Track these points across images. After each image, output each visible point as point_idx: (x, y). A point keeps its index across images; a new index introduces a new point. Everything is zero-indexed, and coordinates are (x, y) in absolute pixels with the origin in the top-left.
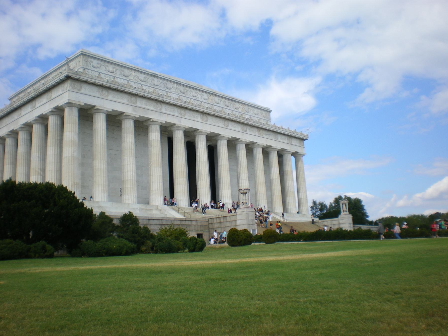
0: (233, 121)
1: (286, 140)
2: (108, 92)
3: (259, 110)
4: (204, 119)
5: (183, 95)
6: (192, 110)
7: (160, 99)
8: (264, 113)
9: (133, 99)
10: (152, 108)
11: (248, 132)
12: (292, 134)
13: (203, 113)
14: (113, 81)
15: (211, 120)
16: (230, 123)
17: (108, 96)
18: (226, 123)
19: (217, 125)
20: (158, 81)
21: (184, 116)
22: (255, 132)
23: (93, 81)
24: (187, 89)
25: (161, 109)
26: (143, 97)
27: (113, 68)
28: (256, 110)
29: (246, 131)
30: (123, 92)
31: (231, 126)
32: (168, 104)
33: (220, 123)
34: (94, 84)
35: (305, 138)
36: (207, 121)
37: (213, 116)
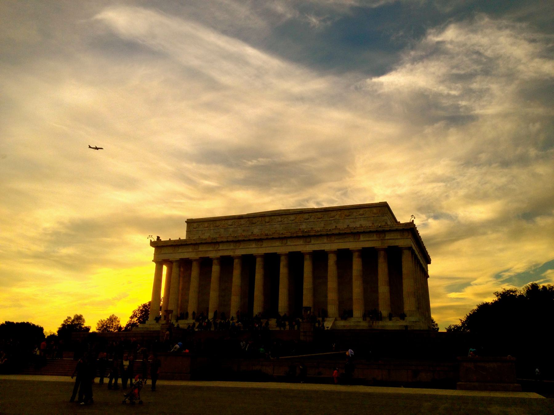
0: (291, 237)
3: (367, 209)
6: (244, 241)
8: (375, 210)
10: (211, 249)
11: (313, 242)
15: (265, 244)
18: (284, 241)
19: (274, 245)
23: (166, 244)
24: (273, 217)
26: (201, 243)
29: (310, 242)
31: (289, 243)
34: (167, 246)
36: (262, 245)
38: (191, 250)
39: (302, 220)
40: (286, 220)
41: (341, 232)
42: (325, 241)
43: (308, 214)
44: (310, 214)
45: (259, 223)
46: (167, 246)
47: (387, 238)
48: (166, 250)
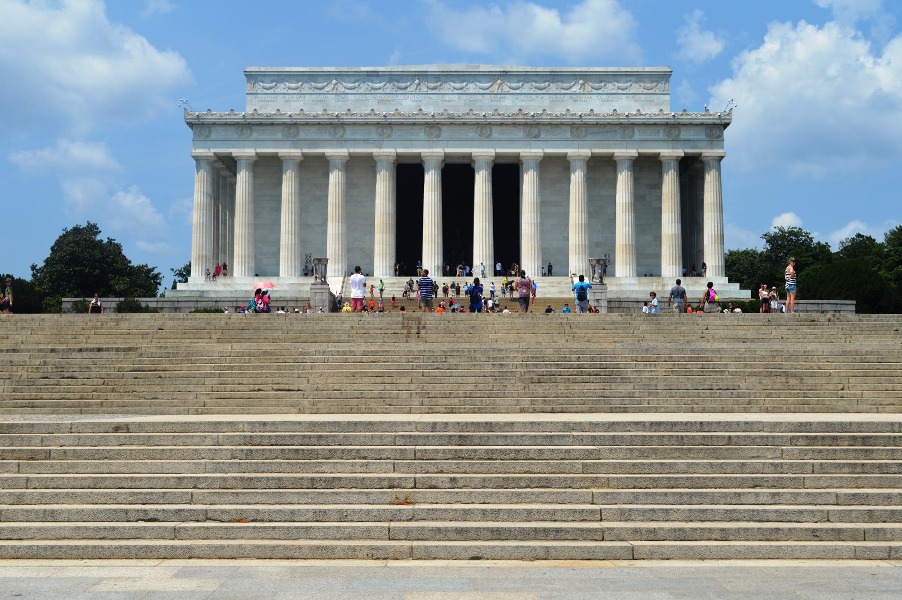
2: (251, 130)
5: (433, 92)
9: (292, 130)
10: (326, 137)
11: (543, 135)
14: (253, 115)
16: (494, 128)
17: (251, 135)
18: (486, 131)
19: (464, 137)
21: (389, 136)
30: (272, 124)
32: (354, 124)
35: (718, 122)
36: (438, 136)
37: (451, 124)
38: (279, 136)
42: (568, 135)
46: (226, 124)
47: (682, 137)
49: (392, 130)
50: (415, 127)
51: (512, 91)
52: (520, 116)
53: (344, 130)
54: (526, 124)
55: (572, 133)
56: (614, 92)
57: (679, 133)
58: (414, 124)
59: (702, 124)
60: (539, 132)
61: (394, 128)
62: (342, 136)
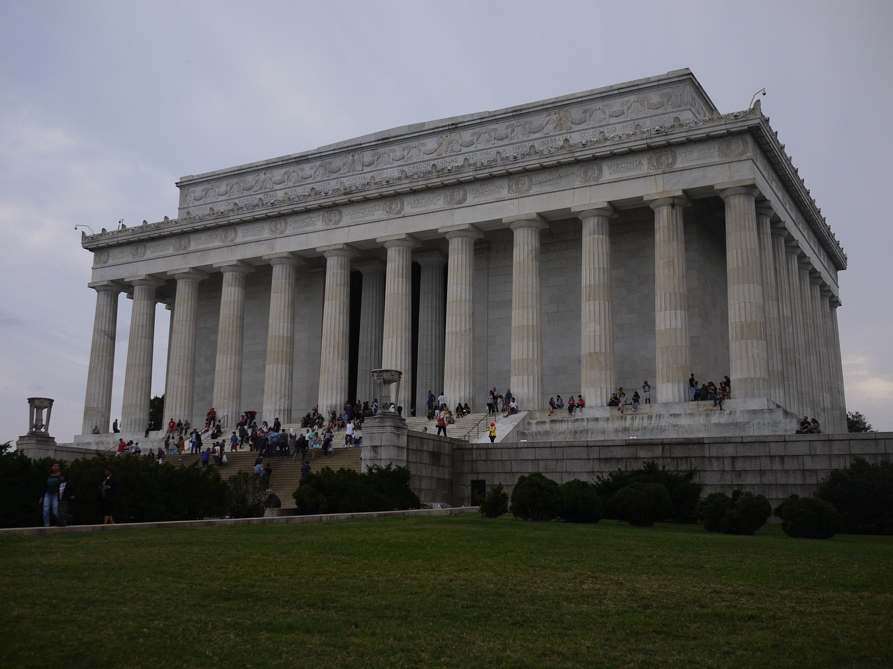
0: (413, 192)
1: (644, 165)
2: (145, 248)
3: (632, 98)
4: (331, 220)
5: (369, 169)
6: (294, 213)
7: (223, 221)
8: (654, 97)
9: (184, 241)
10: (217, 243)
11: (470, 200)
12: (659, 140)
13: (321, 208)
14: (142, 227)
15: (348, 216)
18: (396, 205)
20: (311, 169)
21: (282, 232)
22: (503, 190)
24: (381, 150)
25: (232, 241)
26: (196, 231)
27: (227, 185)
28: (616, 104)
29: (465, 199)
31: (409, 206)
32: (243, 223)
33: (378, 212)
34: (120, 245)
36: (339, 221)
39: (457, 147)
40: (414, 152)
41: (547, 162)
42: (505, 193)
43: (470, 132)
44: (477, 130)
45: (346, 169)
46: (120, 245)
47: (679, 165)
48: (116, 257)
49: (286, 223)
50: (312, 215)
51: (464, 150)
52: (435, 174)
53: (236, 232)
54: (444, 187)
55: (510, 188)
56: (604, 123)
57: (674, 162)
58: (308, 211)
59: (709, 139)
60: (465, 194)
61: (290, 220)
62: (232, 241)
